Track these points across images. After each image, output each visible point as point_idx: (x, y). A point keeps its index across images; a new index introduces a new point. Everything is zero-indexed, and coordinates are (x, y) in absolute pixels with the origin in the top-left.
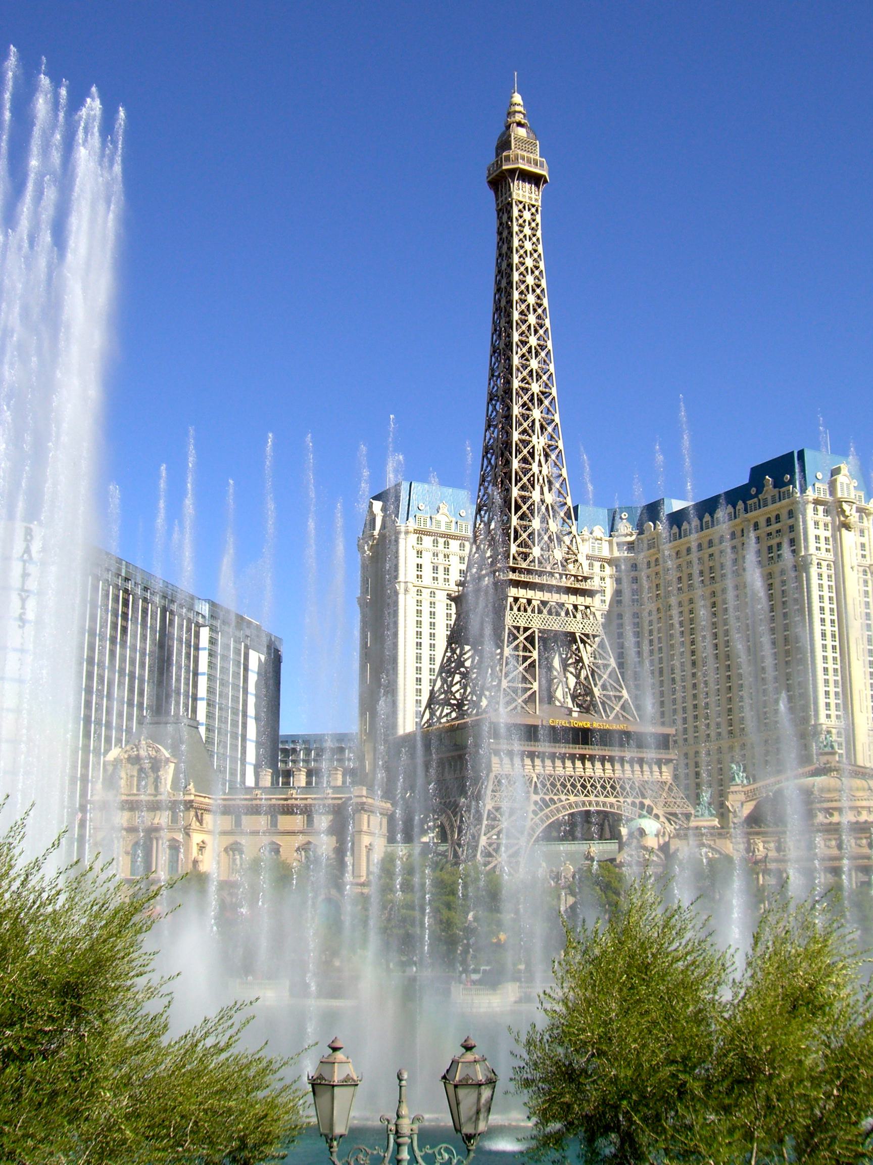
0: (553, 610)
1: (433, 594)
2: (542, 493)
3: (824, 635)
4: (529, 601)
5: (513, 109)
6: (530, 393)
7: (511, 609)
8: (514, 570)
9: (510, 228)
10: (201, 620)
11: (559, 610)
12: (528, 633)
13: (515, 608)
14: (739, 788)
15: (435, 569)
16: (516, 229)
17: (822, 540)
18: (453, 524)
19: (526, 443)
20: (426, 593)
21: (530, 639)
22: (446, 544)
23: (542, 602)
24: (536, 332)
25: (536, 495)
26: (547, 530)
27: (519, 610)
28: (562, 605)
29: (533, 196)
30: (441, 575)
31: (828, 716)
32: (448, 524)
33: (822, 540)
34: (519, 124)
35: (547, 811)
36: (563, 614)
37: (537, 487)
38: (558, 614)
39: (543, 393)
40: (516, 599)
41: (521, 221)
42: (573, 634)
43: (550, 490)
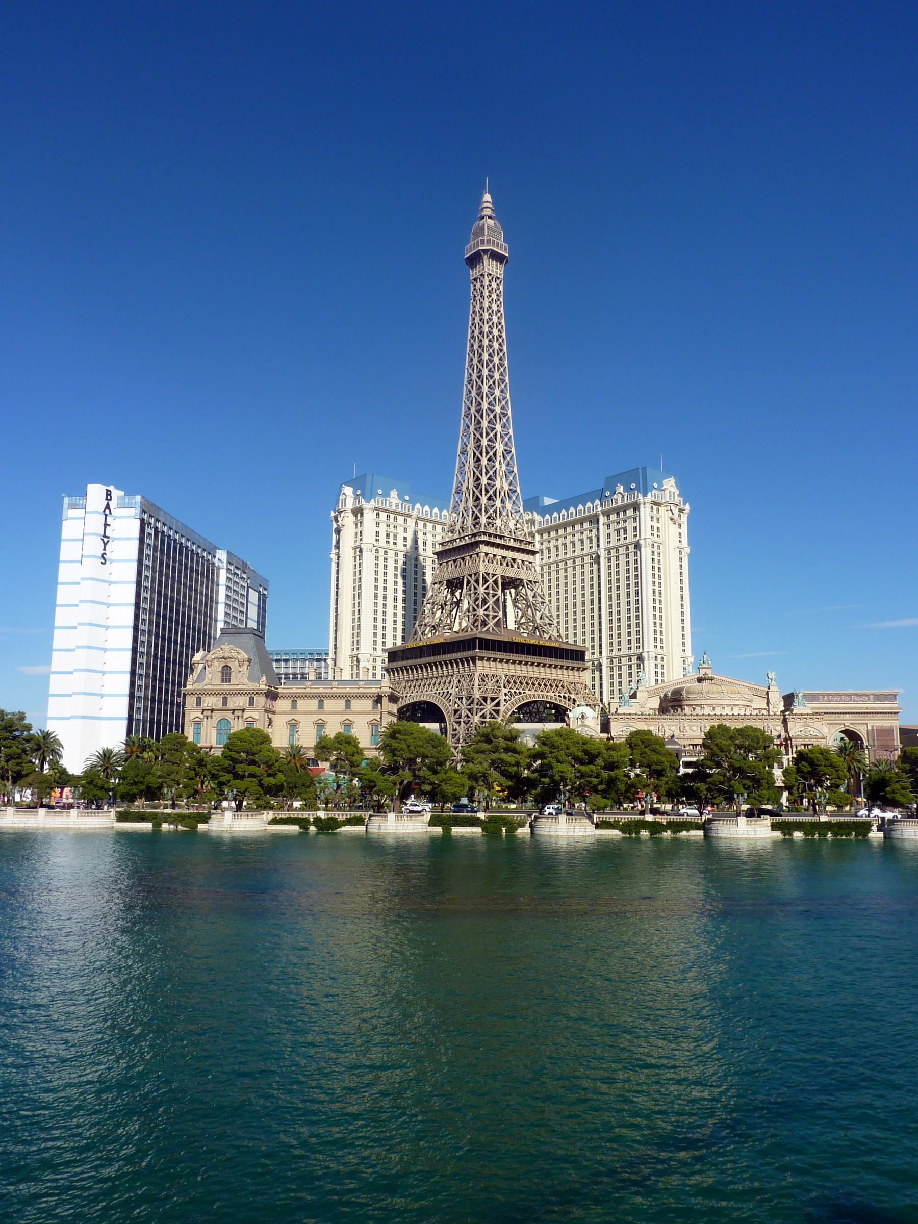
1: (386, 553)
3: (654, 592)
8: (485, 533)
10: (220, 564)
14: (644, 688)
15: (388, 535)
17: (655, 529)
20: (381, 551)
21: (496, 582)
22: (395, 518)
25: (498, 484)
28: (514, 560)
30: (391, 540)
31: (656, 647)
32: (397, 505)
33: (655, 529)
34: (490, 217)
36: (515, 566)
37: (499, 478)
38: (512, 566)
40: (487, 554)
42: (522, 580)
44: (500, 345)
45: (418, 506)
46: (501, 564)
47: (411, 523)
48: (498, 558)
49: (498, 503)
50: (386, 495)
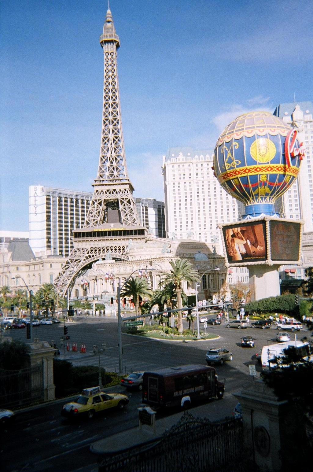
0: (111, 192)
1: (179, 183)
2: (111, 153)
11: (114, 192)
12: (100, 201)
15: (180, 175)
18: (185, 159)
21: (100, 204)
25: (109, 155)
28: (115, 190)
30: (182, 176)
32: (183, 159)
34: (109, 22)
35: (89, 259)
36: (115, 193)
37: (110, 152)
38: (113, 193)
40: (97, 191)
42: (118, 199)
45: (196, 156)
46: (106, 193)
47: (193, 167)
48: (104, 191)
50: (177, 155)
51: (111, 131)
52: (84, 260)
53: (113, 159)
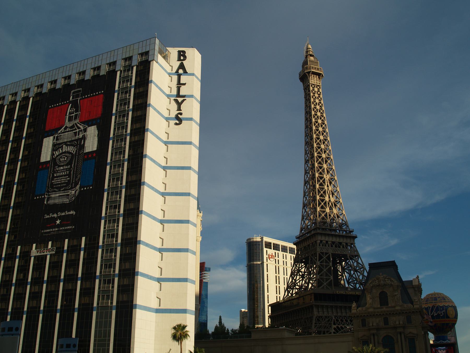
2: (329, 197)
4: (327, 242)
5: (308, 50)
6: (321, 158)
7: (319, 245)
9: (309, 94)
13: (321, 245)
16: (312, 94)
19: (321, 178)
23: (332, 242)
24: (323, 134)
25: (327, 199)
26: (333, 212)
27: (323, 245)
28: (340, 243)
29: (318, 82)
34: (311, 55)
36: (341, 247)
38: (339, 247)
39: (328, 158)
40: (321, 241)
41: (313, 92)
43: (333, 196)
44: (322, 120)
46: (332, 246)
49: (328, 210)
51: (326, 170)
52: (334, 333)
53: (332, 204)
